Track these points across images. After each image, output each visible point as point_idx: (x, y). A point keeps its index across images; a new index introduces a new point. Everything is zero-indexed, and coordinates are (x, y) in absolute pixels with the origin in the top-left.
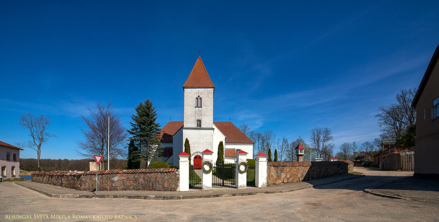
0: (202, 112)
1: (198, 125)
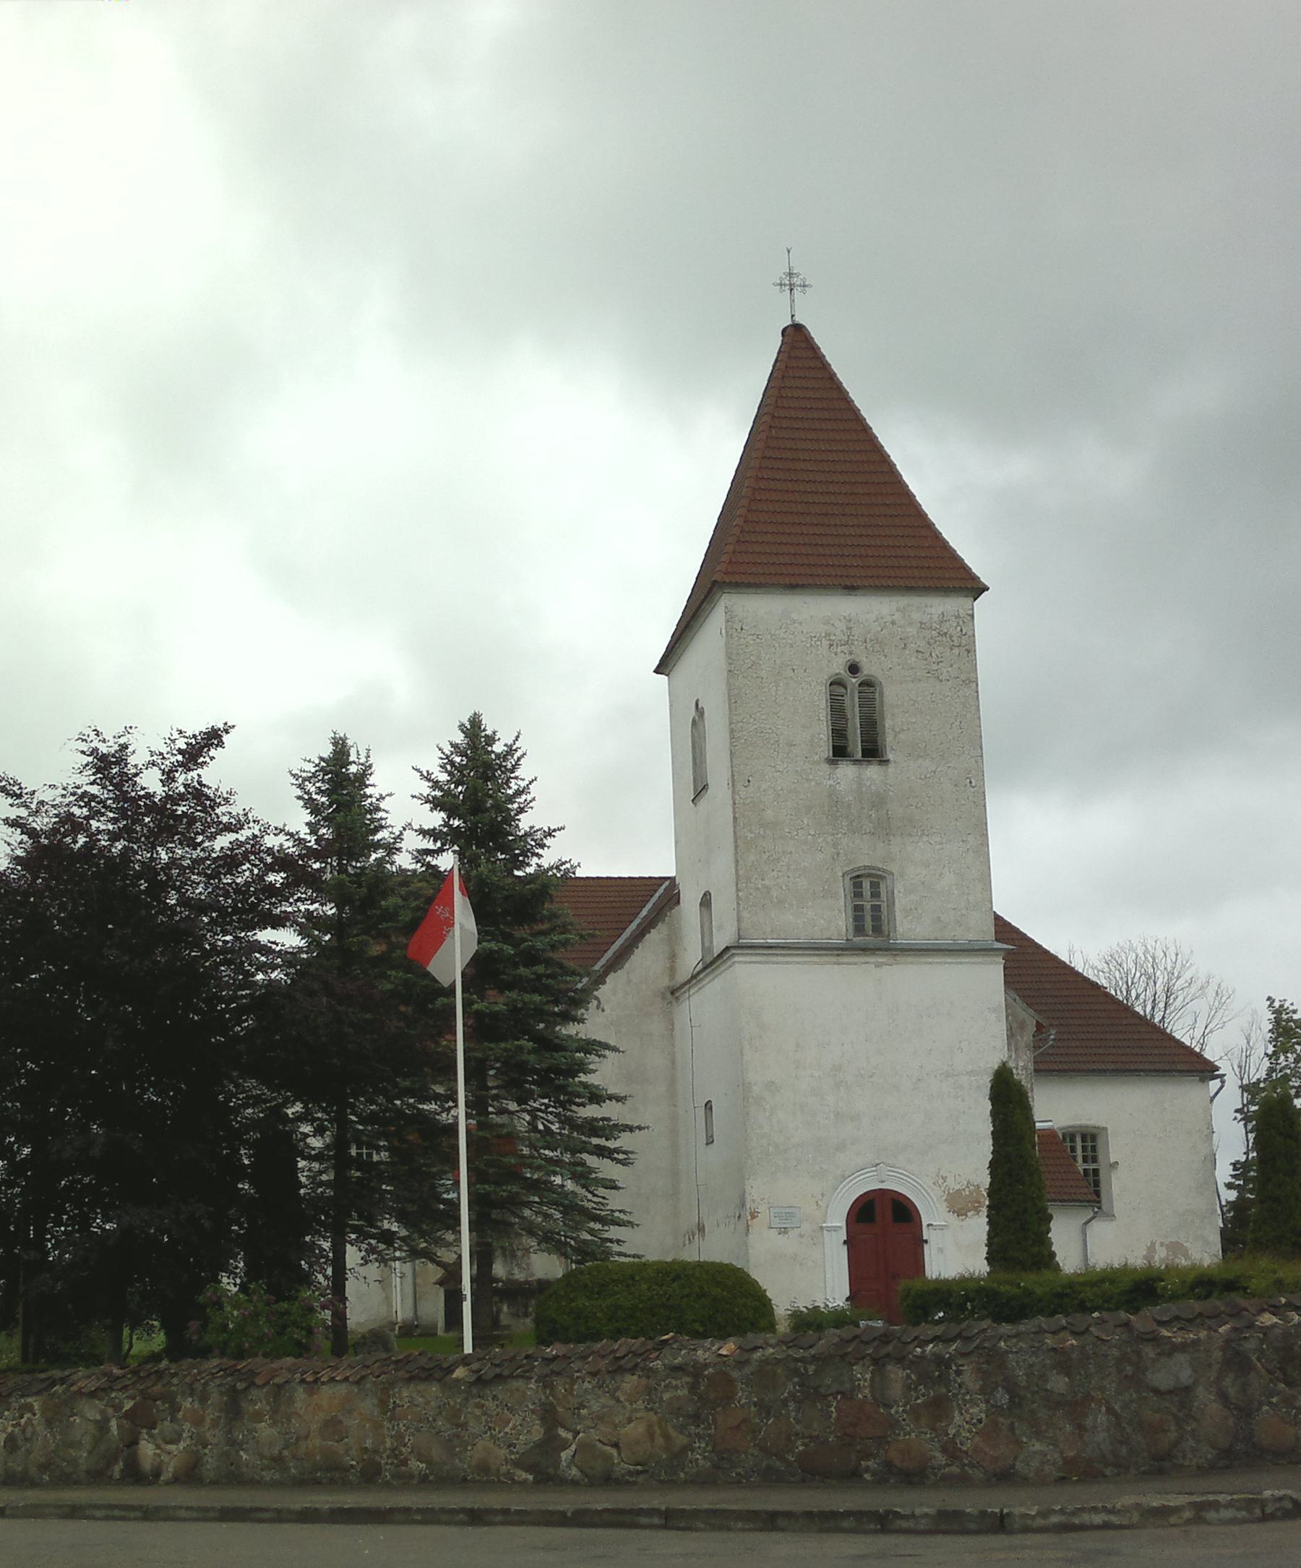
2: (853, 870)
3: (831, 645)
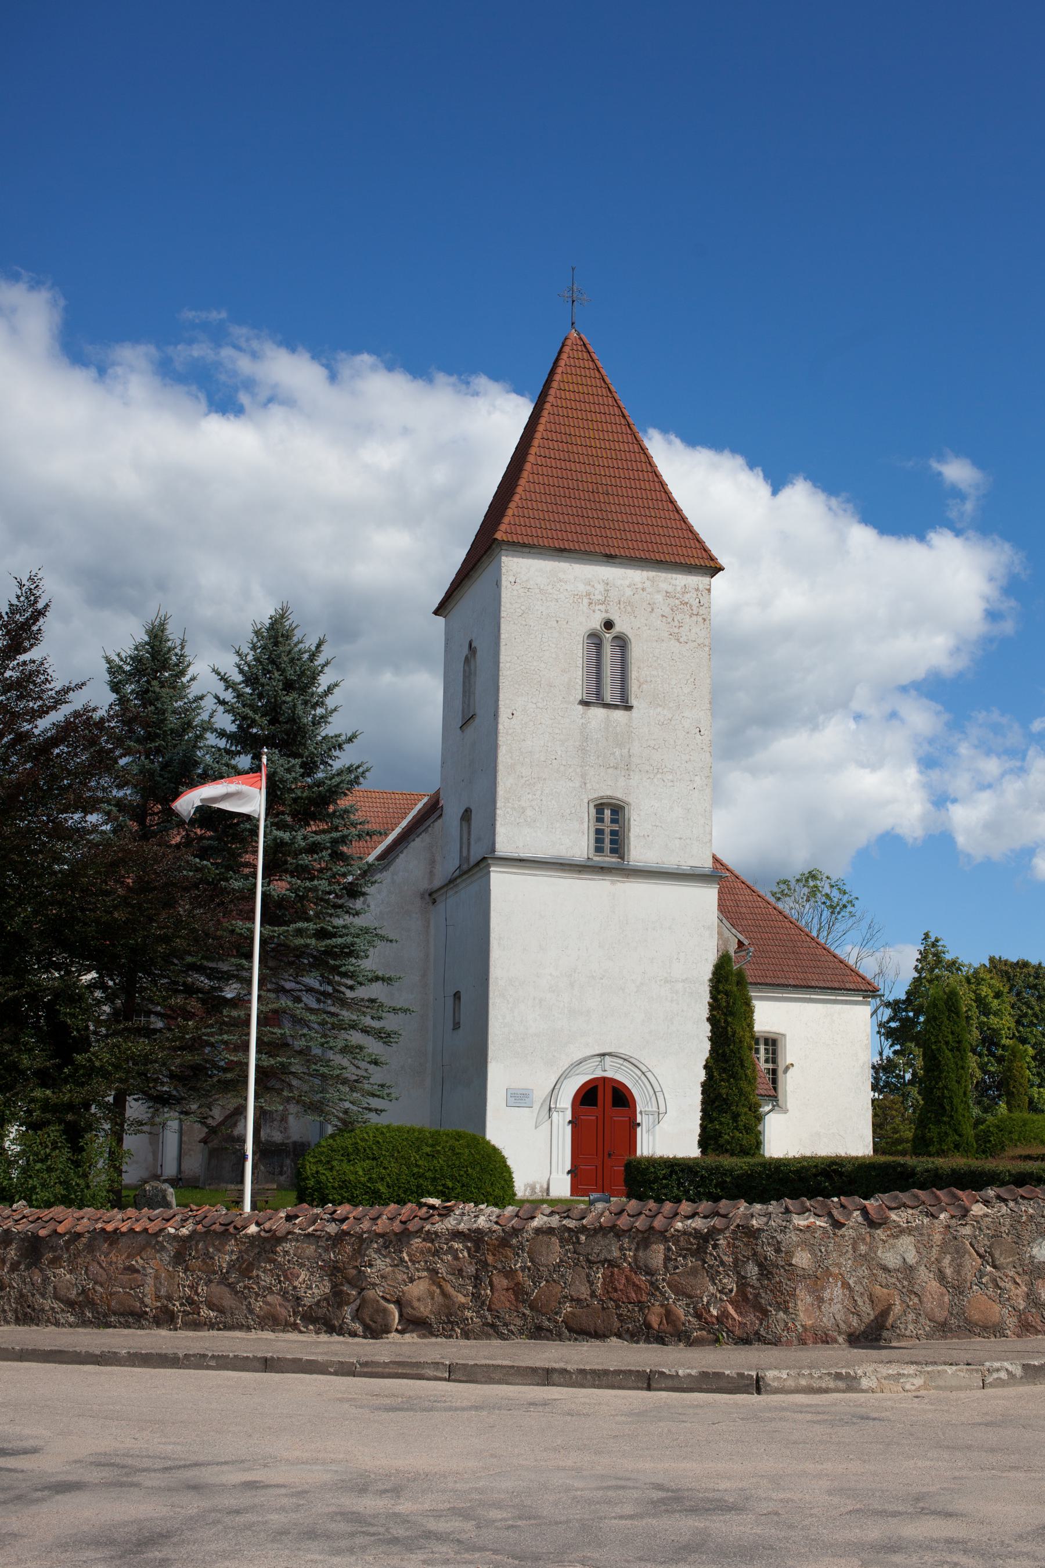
1: (599, 839)
2: (597, 799)
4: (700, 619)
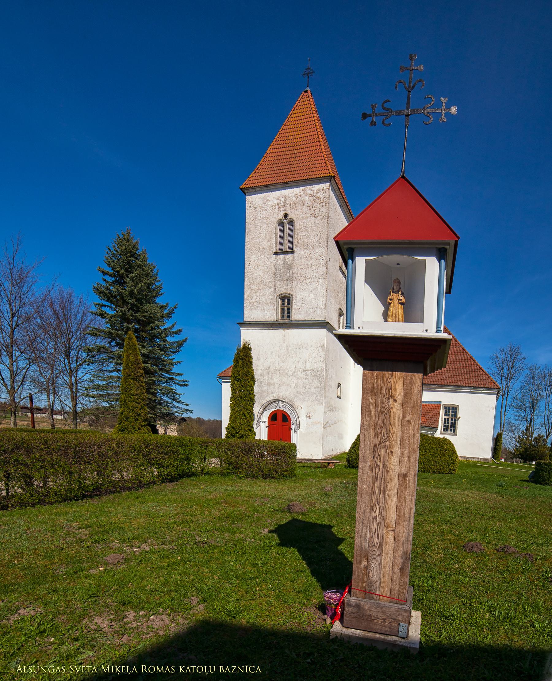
0: (295, 271)
1: (283, 313)
3: (279, 208)
4: (324, 204)
